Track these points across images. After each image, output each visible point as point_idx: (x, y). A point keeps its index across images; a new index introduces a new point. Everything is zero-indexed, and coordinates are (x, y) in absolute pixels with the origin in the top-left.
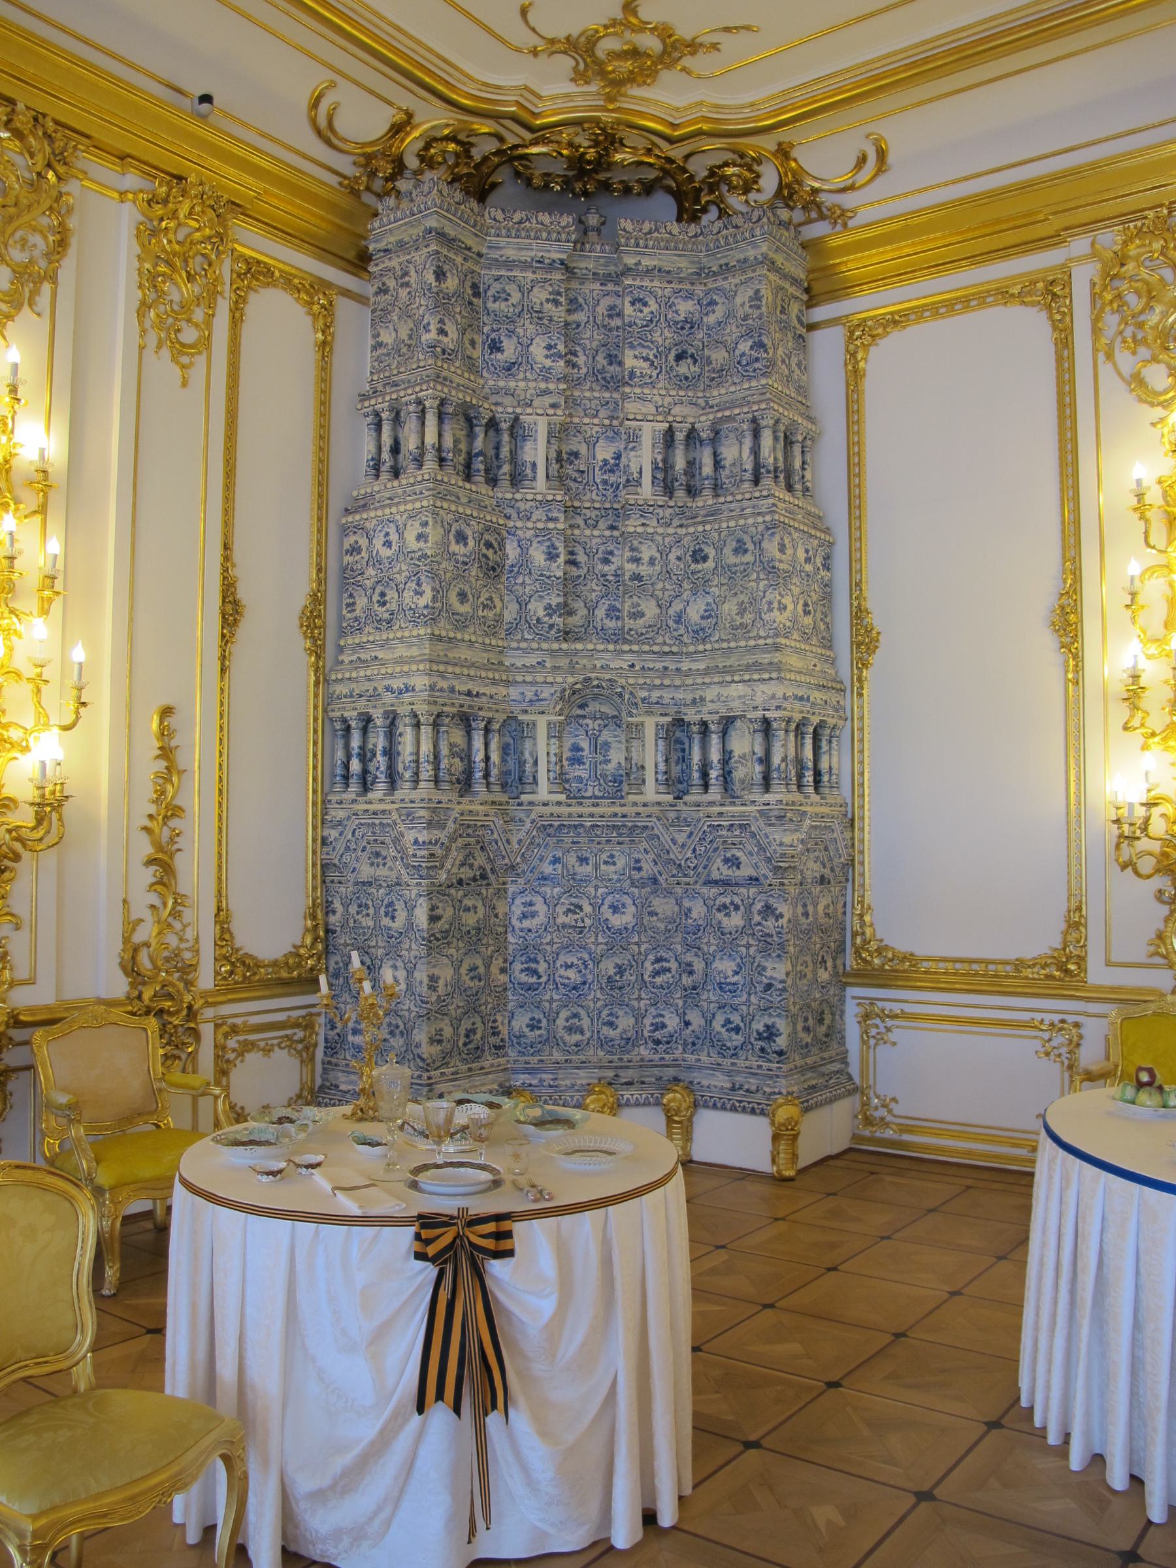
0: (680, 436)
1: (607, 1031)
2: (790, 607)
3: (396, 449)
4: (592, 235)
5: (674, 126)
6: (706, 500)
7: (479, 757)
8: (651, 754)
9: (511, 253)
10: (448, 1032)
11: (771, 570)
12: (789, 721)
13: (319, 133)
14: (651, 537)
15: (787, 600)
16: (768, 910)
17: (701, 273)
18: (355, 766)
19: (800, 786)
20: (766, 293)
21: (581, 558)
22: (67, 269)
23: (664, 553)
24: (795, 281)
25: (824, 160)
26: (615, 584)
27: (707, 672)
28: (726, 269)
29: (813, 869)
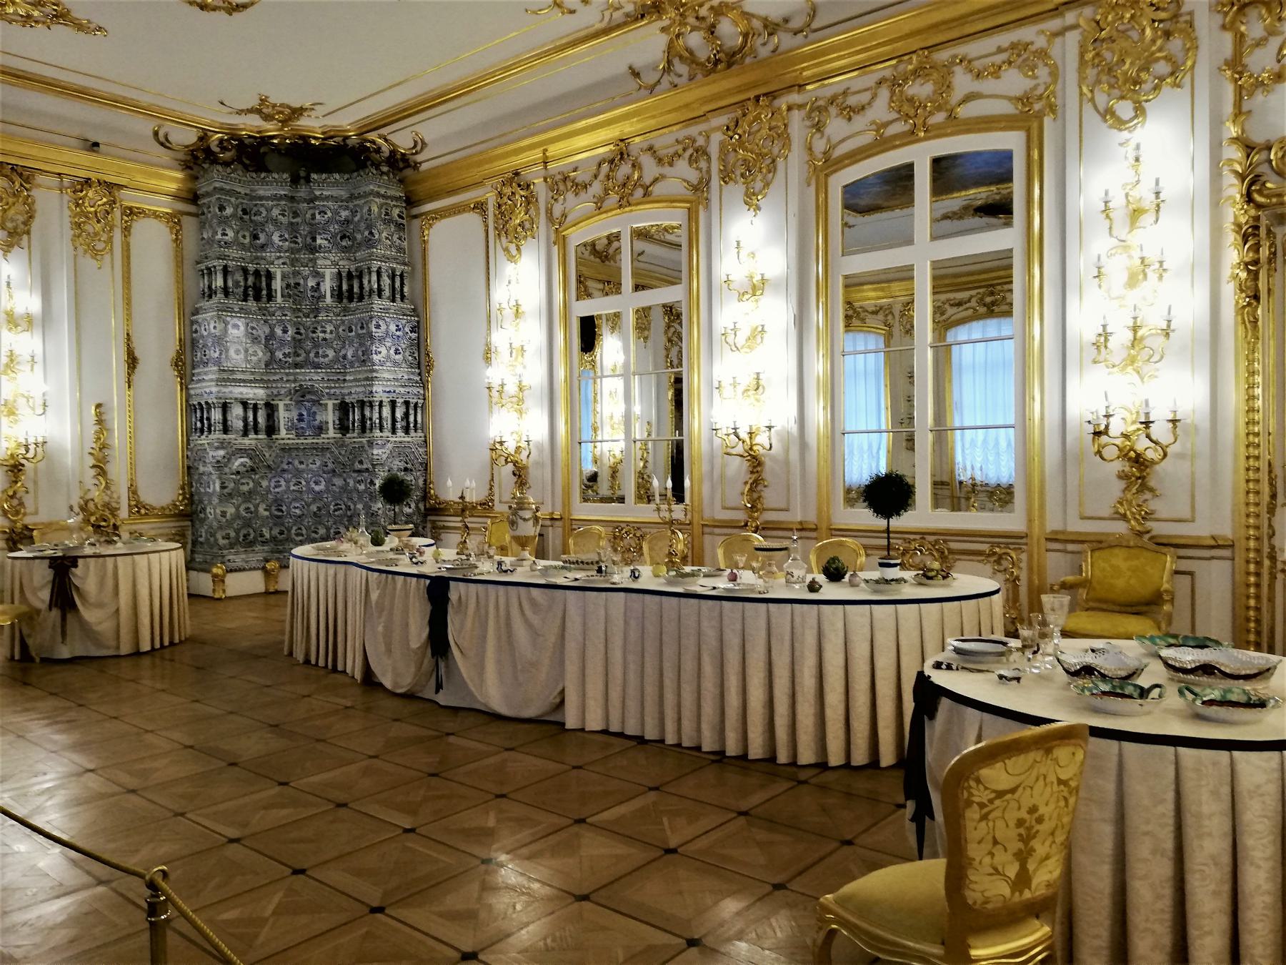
0: (344, 275)
1: (314, 535)
2: (384, 351)
3: (210, 287)
4: (302, 181)
5: (323, 133)
6: (353, 305)
7: (251, 419)
8: (329, 416)
9: (261, 193)
10: (233, 534)
11: (371, 337)
12: (381, 402)
13: (162, 144)
14: (330, 321)
15: (384, 351)
16: (372, 483)
17: (352, 197)
18: (199, 425)
19: (394, 431)
20: (375, 209)
21: (302, 331)
22: (35, 226)
23: (337, 328)
24: (397, 199)
25: (403, 140)
26: (316, 345)
27: (355, 380)
28: (359, 197)
29: (397, 464)
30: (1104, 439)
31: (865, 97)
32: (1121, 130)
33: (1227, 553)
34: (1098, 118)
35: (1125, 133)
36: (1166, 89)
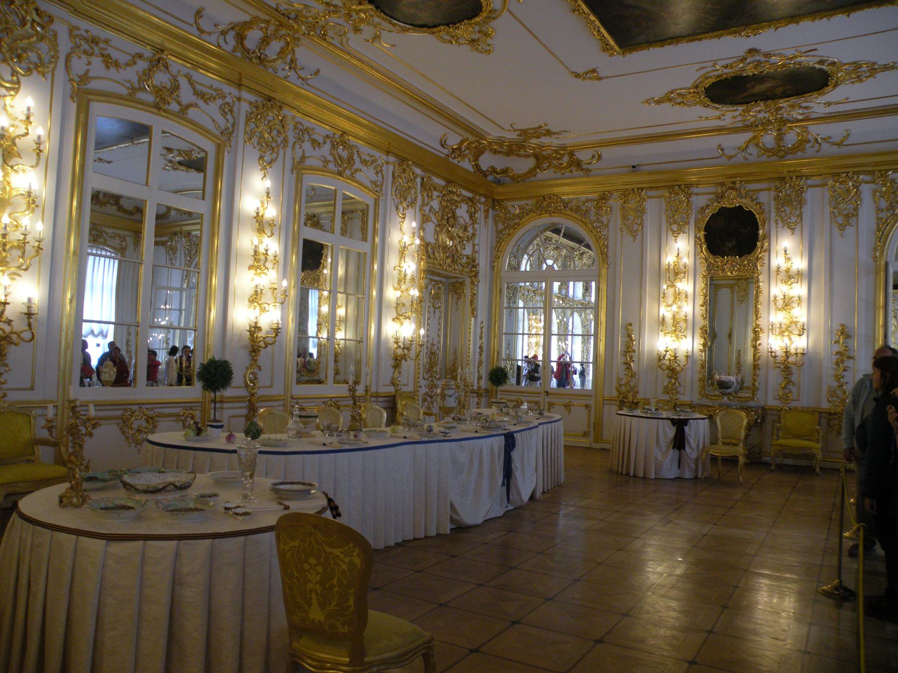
31: (321, 140)
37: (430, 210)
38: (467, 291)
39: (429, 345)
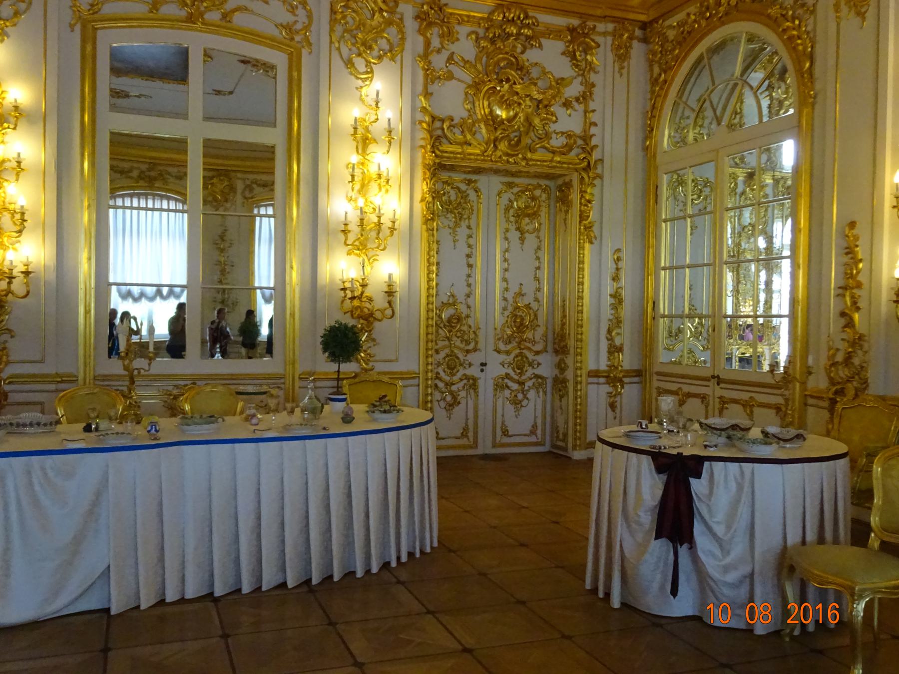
30: (356, 303)
32: (358, 78)
33: (415, 382)
34: (342, 64)
35: (360, 81)
36: (386, 60)
37: (450, 59)
38: (575, 196)
39: (510, 296)
